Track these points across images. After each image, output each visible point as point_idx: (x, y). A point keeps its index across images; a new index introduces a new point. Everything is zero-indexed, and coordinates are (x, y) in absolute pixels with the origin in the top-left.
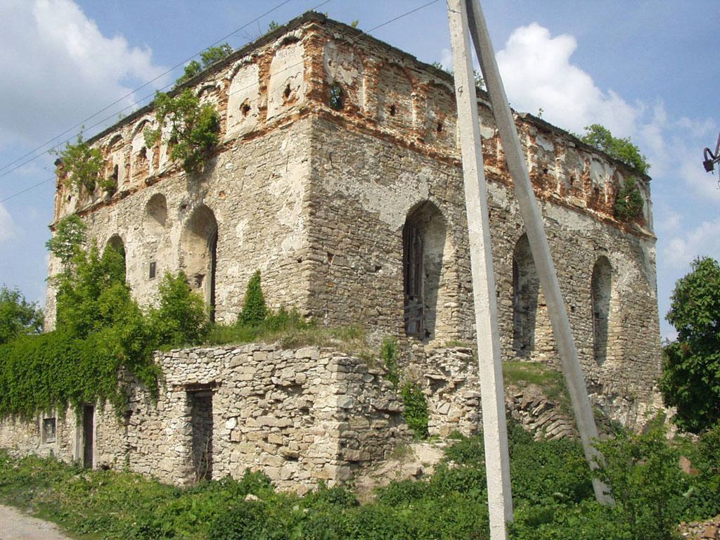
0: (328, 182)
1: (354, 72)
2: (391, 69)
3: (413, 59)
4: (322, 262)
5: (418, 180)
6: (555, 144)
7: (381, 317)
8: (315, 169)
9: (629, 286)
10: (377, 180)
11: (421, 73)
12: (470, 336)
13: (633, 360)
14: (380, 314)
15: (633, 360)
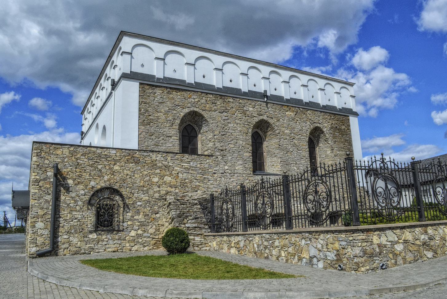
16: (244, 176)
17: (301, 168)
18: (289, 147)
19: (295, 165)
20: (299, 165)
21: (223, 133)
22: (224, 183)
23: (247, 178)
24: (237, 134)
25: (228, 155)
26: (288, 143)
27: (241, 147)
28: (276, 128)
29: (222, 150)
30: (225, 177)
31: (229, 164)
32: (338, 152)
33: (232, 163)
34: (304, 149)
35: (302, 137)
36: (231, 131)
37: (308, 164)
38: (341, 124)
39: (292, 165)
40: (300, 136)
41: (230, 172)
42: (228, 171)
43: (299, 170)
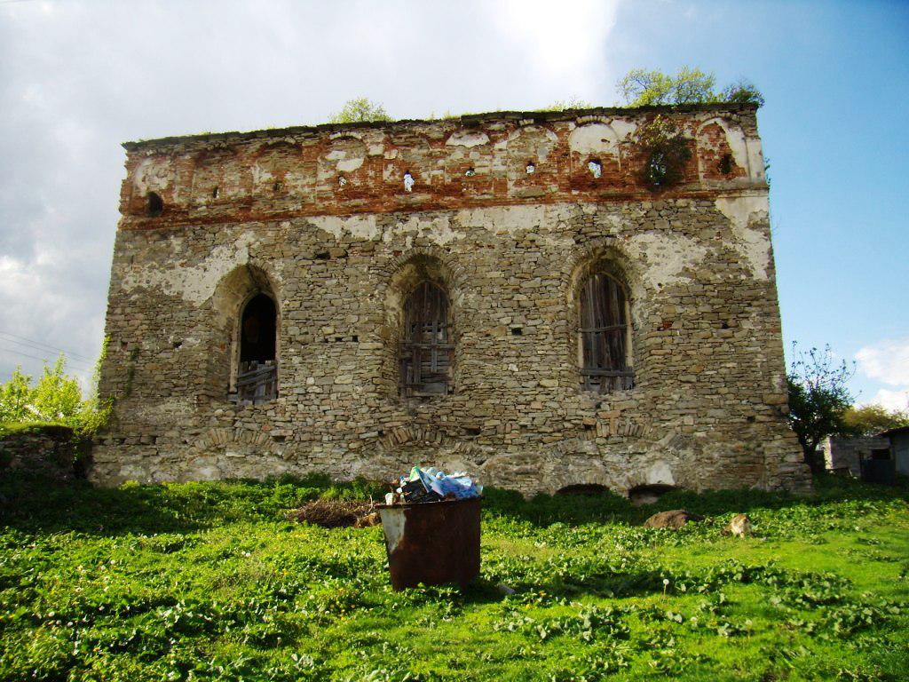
0: (127, 283)
1: (171, 176)
2: (215, 155)
3: (237, 134)
4: (115, 352)
5: (236, 249)
6: (489, 133)
7: (176, 389)
8: (116, 274)
9: (679, 275)
10: (182, 265)
11: (249, 143)
12: (302, 391)
13: (688, 382)
14: (175, 386)
15: (688, 382)
16: (356, 397)
17: (533, 365)
18: (499, 315)
19: (513, 359)
20: (529, 359)
21: (306, 304)
22: (301, 416)
23: (363, 401)
24: (345, 300)
25: (317, 352)
26: (494, 305)
27: (351, 331)
28: (459, 269)
29: (304, 343)
30: (306, 403)
31: (318, 372)
32: (679, 310)
33: (328, 371)
34: (549, 315)
35: (545, 283)
36: (329, 296)
37: (561, 353)
38: (698, 225)
39: (505, 360)
40: (539, 279)
41: (318, 390)
42: (315, 387)
43: (525, 373)
